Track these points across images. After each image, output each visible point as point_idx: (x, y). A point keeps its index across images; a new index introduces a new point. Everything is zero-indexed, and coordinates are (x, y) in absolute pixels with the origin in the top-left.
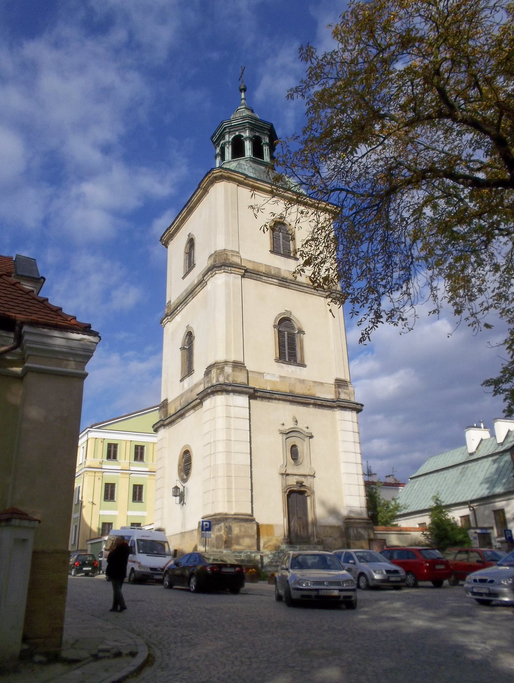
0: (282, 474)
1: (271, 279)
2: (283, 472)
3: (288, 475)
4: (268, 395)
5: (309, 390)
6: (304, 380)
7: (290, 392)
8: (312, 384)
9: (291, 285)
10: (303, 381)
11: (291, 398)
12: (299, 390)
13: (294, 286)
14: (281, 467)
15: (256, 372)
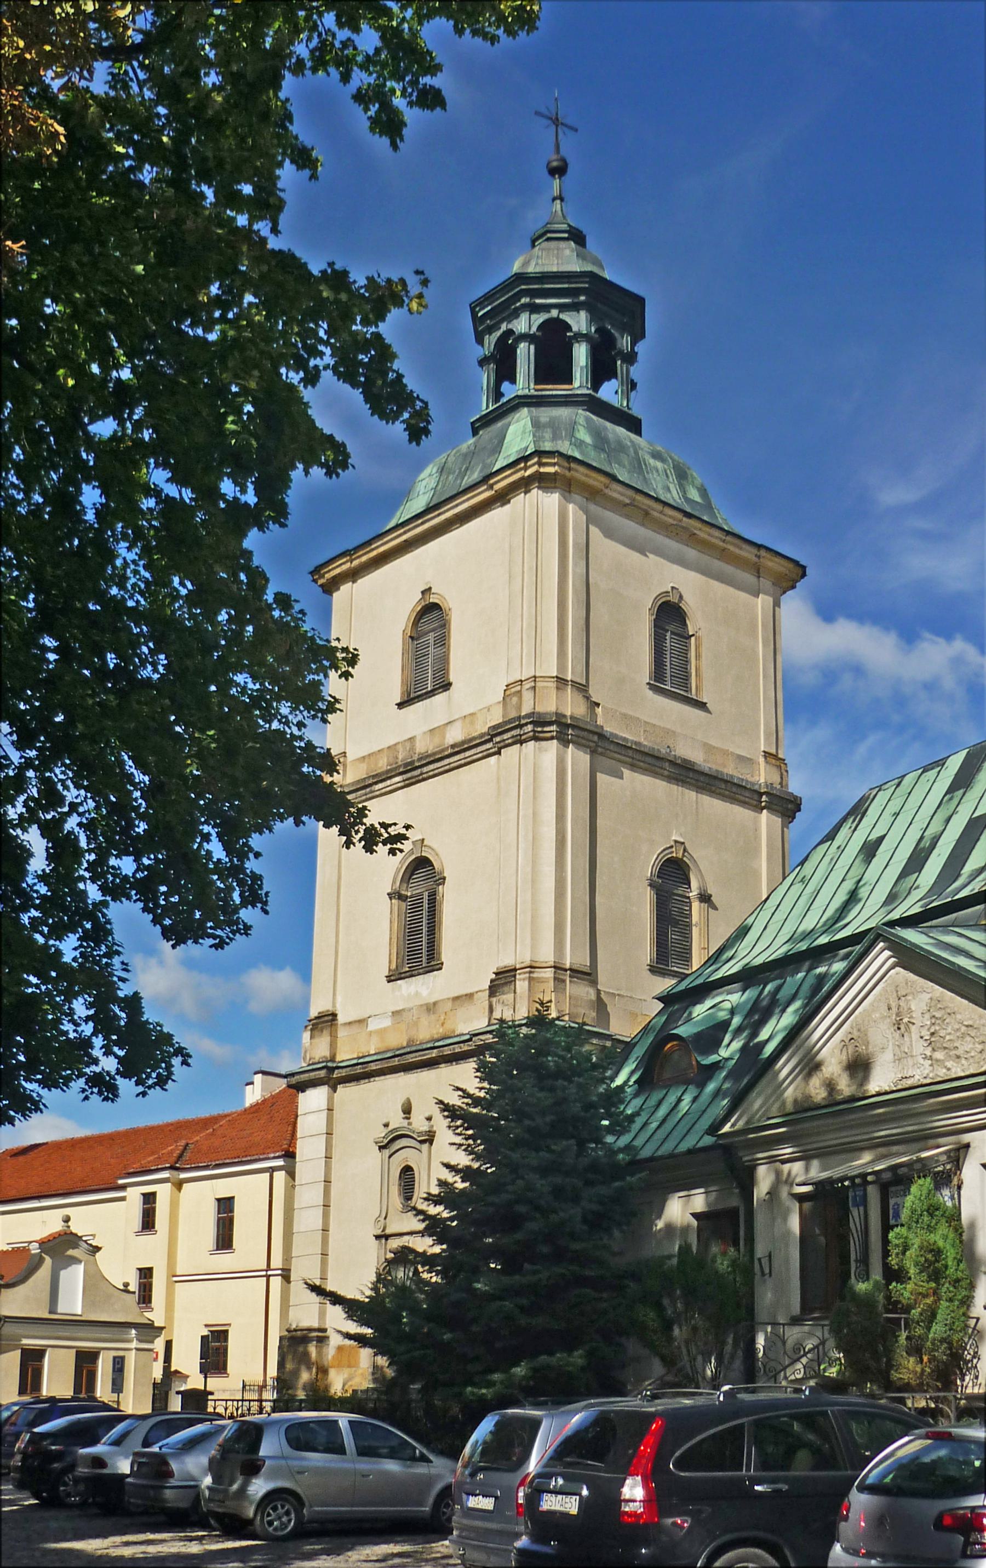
0: (378, 1237)
1: (388, 782)
2: (379, 1232)
3: (387, 1237)
4: (359, 1070)
5: (443, 1024)
6: (435, 1004)
7: (408, 1046)
8: (450, 1004)
9: (425, 769)
10: (431, 1008)
11: (396, 1062)
12: (426, 1031)
13: (431, 767)
14: (377, 1221)
15: (355, 1022)
